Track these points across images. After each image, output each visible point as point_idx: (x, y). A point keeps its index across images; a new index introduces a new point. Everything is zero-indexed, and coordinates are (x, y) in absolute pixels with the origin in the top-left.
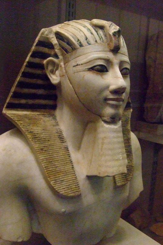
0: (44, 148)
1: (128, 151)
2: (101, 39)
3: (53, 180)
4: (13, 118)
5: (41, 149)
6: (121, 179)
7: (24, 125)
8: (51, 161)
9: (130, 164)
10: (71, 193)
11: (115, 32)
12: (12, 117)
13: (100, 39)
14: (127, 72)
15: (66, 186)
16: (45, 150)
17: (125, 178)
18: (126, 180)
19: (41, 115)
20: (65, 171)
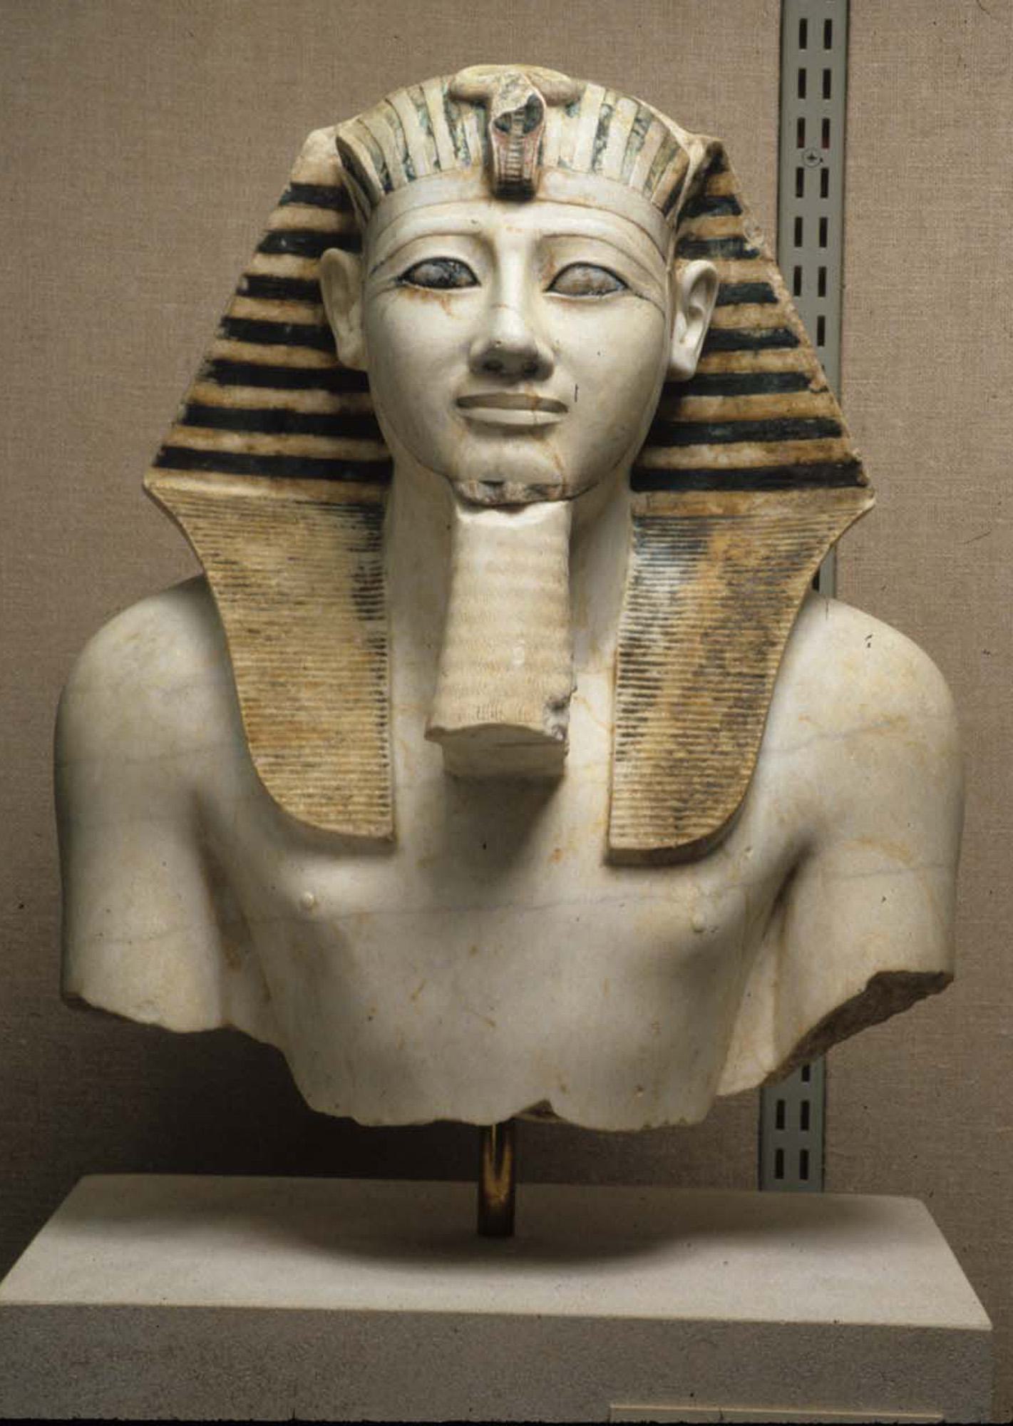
0: (264, 627)
2: (463, 150)
3: (267, 756)
4: (174, 507)
5: (250, 631)
7: (206, 535)
8: (282, 680)
9: (728, 764)
10: (338, 822)
11: (506, 116)
12: (169, 501)
13: (457, 150)
14: (590, 280)
15: (324, 788)
16: (269, 638)
17: (671, 821)
18: (671, 830)
20: (338, 733)
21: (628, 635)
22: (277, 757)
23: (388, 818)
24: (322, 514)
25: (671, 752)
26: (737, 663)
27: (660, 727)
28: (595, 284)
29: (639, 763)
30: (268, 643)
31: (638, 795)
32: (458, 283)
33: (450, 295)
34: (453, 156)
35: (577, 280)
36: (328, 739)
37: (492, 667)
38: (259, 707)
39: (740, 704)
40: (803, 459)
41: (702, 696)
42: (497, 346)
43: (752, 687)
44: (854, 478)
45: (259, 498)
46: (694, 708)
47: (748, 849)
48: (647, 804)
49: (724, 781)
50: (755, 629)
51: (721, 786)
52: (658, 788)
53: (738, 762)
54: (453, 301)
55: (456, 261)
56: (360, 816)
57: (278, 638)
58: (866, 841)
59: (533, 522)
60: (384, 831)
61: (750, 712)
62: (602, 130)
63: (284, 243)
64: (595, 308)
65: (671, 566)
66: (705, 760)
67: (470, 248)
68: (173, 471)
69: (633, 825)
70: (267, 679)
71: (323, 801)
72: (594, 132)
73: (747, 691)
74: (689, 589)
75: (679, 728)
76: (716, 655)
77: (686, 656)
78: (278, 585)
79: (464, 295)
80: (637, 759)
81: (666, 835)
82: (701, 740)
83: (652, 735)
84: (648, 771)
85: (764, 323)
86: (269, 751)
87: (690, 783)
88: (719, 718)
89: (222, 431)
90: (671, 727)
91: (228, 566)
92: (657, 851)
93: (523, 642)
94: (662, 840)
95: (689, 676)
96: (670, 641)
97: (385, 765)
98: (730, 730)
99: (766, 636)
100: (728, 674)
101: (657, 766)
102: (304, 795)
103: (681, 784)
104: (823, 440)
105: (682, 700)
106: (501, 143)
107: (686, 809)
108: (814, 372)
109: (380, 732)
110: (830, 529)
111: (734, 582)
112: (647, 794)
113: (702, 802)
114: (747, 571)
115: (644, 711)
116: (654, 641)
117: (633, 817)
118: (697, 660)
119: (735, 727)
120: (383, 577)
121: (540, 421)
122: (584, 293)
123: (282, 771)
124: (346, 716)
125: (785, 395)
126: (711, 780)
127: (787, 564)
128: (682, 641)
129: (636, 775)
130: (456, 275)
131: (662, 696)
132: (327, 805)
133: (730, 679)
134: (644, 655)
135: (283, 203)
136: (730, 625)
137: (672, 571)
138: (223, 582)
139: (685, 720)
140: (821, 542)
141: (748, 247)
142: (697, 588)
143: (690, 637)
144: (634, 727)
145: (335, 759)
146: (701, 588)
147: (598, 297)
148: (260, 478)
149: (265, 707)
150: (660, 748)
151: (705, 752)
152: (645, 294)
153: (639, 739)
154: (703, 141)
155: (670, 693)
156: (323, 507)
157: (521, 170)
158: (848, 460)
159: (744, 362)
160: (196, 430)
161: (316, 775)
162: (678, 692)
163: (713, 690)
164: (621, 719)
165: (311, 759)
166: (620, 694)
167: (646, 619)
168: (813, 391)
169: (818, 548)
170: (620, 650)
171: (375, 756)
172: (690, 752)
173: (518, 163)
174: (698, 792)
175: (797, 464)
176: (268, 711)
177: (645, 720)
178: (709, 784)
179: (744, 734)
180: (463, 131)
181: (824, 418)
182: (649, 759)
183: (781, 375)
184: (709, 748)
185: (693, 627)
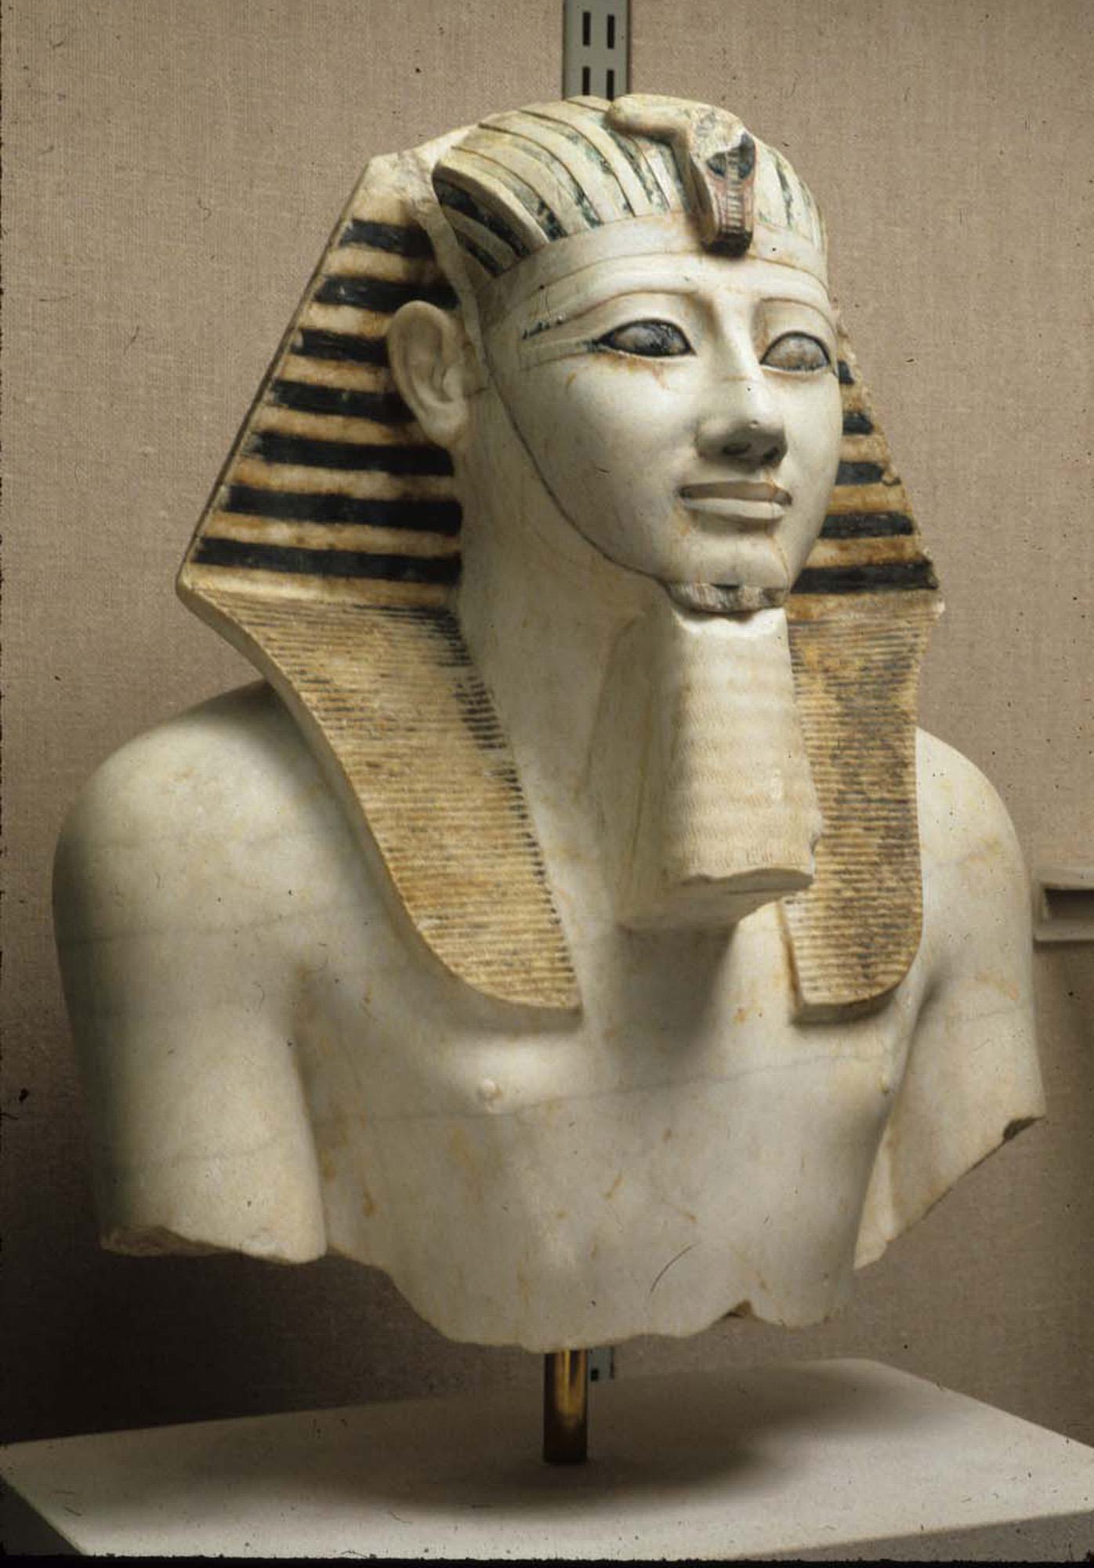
0: (383, 759)
1: (887, 828)
3: (430, 917)
5: (370, 765)
7: (282, 648)
8: (421, 823)
9: (898, 901)
11: (719, 156)
12: (224, 605)
13: (649, 193)
14: (805, 353)
15: (500, 952)
17: (859, 969)
18: (862, 980)
20: (498, 885)
25: (838, 891)
26: (877, 788)
28: (809, 358)
29: (810, 905)
30: (393, 779)
32: (671, 351)
33: (662, 364)
34: (646, 199)
35: (793, 352)
36: (488, 894)
37: (753, 802)
38: (405, 858)
39: (891, 833)
40: (876, 558)
41: (850, 826)
42: (754, 426)
43: (899, 814)
44: (925, 579)
45: (314, 602)
46: (849, 841)
48: (830, 951)
49: (900, 921)
51: (896, 926)
52: (836, 932)
53: (906, 900)
54: (666, 371)
55: (669, 325)
57: (402, 774)
58: (982, 978)
59: (768, 632)
61: (904, 842)
63: (342, 292)
64: (806, 385)
66: (874, 899)
67: (682, 309)
68: (216, 568)
69: (824, 977)
71: (504, 968)
73: (896, 819)
75: (839, 863)
76: (851, 778)
78: (381, 708)
79: (677, 365)
80: (808, 901)
84: (820, 913)
86: (430, 911)
87: (866, 925)
88: (875, 849)
89: (270, 520)
90: (831, 862)
91: (321, 686)
92: (851, 1005)
93: (778, 772)
94: (856, 992)
98: (890, 863)
102: (481, 963)
104: (896, 537)
105: (833, 832)
106: (718, 188)
108: (887, 462)
109: (541, 883)
110: (916, 636)
111: (844, 696)
112: (826, 941)
113: (884, 947)
117: (820, 966)
119: (894, 859)
120: (490, 696)
122: (798, 368)
123: (451, 935)
124: (501, 865)
125: (859, 486)
126: (888, 921)
127: (888, 676)
129: (809, 919)
130: (669, 340)
132: (508, 973)
133: (873, 805)
135: (343, 243)
136: (856, 744)
138: (321, 705)
139: (842, 854)
142: (808, 703)
143: (820, 759)
145: (503, 917)
146: (814, 703)
147: (810, 373)
148: (311, 577)
149: (414, 857)
151: (871, 889)
156: (385, 612)
157: (742, 221)
158: (920, 560)
161: (488, 937)
163: (860, 819)
165: (478, 919)
168: (886, 484)
169: (913, 657)
171: (543, 911)
172: (857, 890)
173: (738, 213)
174: (876, 934)
175: (870, 564)
176: (418, 863)
178: (885, 926)
180: (650, 169)
181: (897, 513)
182: (817, 900)
184: (875, 884)
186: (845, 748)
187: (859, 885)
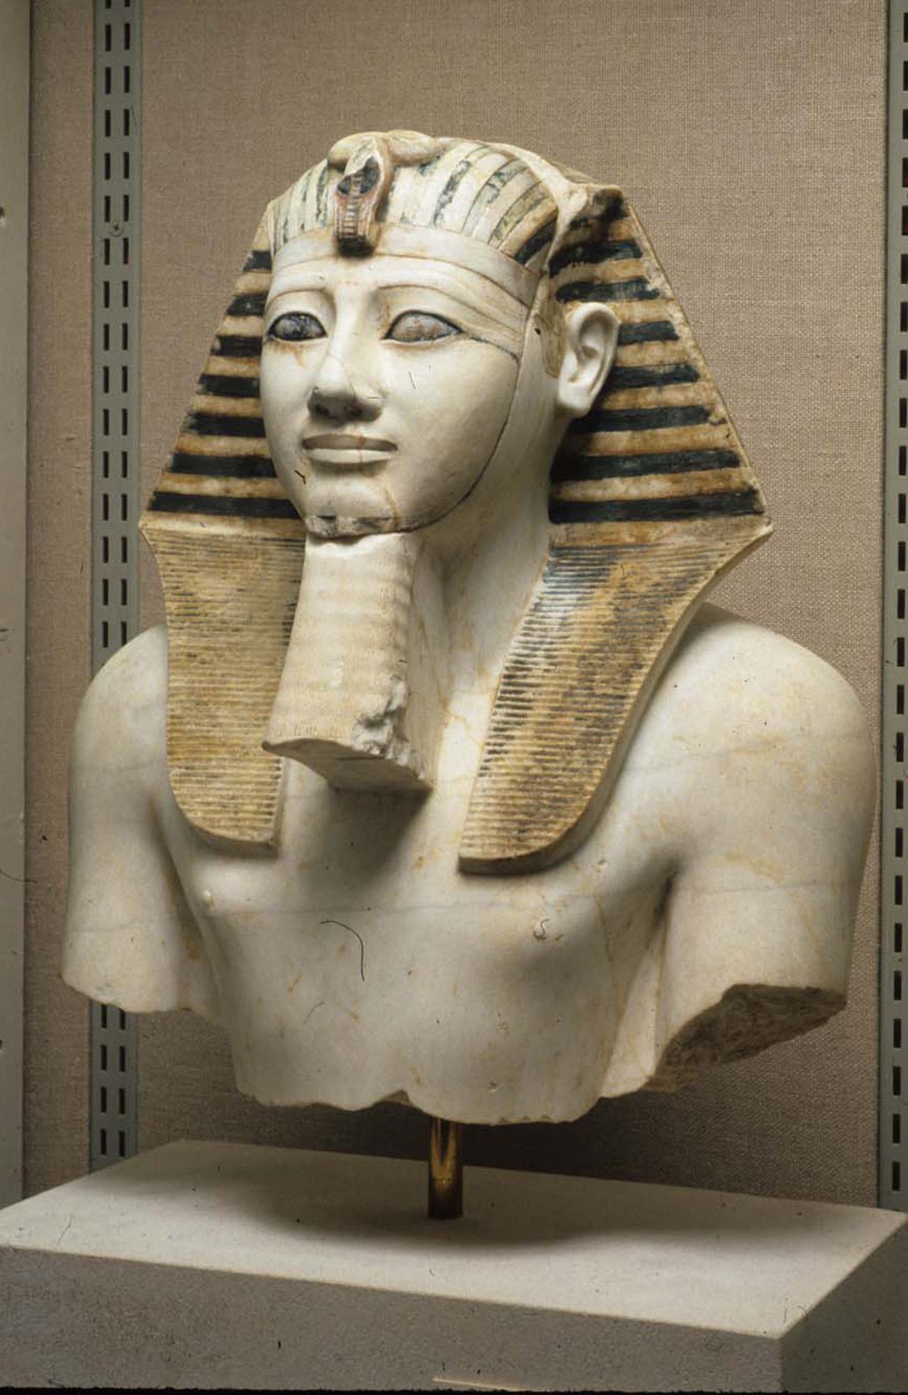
1: (598, 719)
5: (189, 655)
6: (494, 833)
8: (205, 699)
9: (576, 780)
10: (226, 827)
12: (152, 540)
13: (319, 212)
14: (421, 327)
15: (222, 797)
16: (203, 662)
17: (515, 833)
18: (514, 842)
19: (277, 543)
20: (243, 747)
21: (515, 658)
22: (187, 768)
23: (271, 825)
24: (277, 550)
25: (528, 768)
26: (604, 685)
27: (523, 745)
28: (426, 330)
30: (201, 666)
31: (491, 809)
32: (309, 335)
33: (302, 346)
34: (315, 218)
35: (411, 327)
36: (233, 753)
37: (313, 687)
38: (181, 723)
39: (598, 723)
40: (705, 489)
43: (612, 708)
44: (751, 505)
45: (233, 536)
46: (557, 727)
47: (602, 862)
48: (498, 817)
49: (569, 796)
50: (627, 652)
51: (566, 801)
52: (510, 802)
53: (583, 779)
54: (305, 352)
55: (307, 315)
56: (247, 823)
57: (211, 662)
58: (733, 857)
59: (362, 553)
60: (266, 836)
61: (605, 731)
62: (452, 185)
63: (249, 306)
64: (427, 352)
65: (571, 593)
66: (556, 777)
67: (318, 304)
69: (482, 836)
70: (193, 698)
71: (218, 808)
72: (442, 188)
73: (607, 711)
74: (577, 615)
76: (587, 677)
77: (561, 678)
78: (222, 614)
79: (313, 346)
81: (509, 847)
82: (557, 758)
83: (515, 752)
84: (504, 785)
85: (666, 360)
86: (183, 763)
87: (539, 798)
89: (204, 477)
90: (533, 745)
91: (183, 598)
92: (499, 861)
93: (342, 664)
95: (559, 697)
96: (551, 664)
97: (277, 777)
98: (585, 748)
99: (635, 659)
100: (593, 695)
101: (513, 781)
102: (202, 803)
103: (531, 798)
104: (723, 470)
106: (341, 205)
107: (531, 822)
108: (713, 404)
110: (722, 556)
111: (621, 608)
112: (499, 808)
113: (546, 816)
114: (635, 597)
115: (512, 729)
116: (536, 664)
117: (484, 828)
118: (569, 682)
119: (589, 745)
121: (365, 460)
122: (417, 339)
123: (190, 781)
124: (253, 732)
125: (688, 427)
126: (558, 795)
127: (672, 589)
128: (560, 664)
129: (493, 789)
130: (307, 327)
131: (531, 716)
132: (220, 812)
133: (594, 699)
134: (525, 677)
135: (247, 269)
136: (607, 648)
137: (570, 598)
138: (176, 612)
140: (708, 569)
141: (650, 288)
142: (584, 613)
144: (501, 745)
145: (235, 770)
146: (590, 613)
147: (429, 343)
148: (236, 519)
149: (188, 723)
150: (520, 764)
151: (557, 769)
152: (483, 337)
153: (503, 755)
154: (588, 191)
155: (539, 713)
156: (284, 543)
157: (355, 228)
158: (746, 489)
159: (650, 398)
160: (182, 476)
161: (219, 785)
162: (546, 712)
163: (577, 710)
164: (491, 737)
165: (216, 771)
166: (495, 714)
167: (535, 643)
168: (713, 424)
170: (506, 672)
171: (270, 768)
172: (545, 769)
173: (353, 221)
174: (544, 806)
175: (700, 494)
177: (512, 738)
178: (555, 799)
179: (595, 752)
181: (723, 448)
182: (507, 774)
183: (683, 408)
184: (562, 765)
185: (574, 650)
186: (597, 651)
187: (547, 765)
